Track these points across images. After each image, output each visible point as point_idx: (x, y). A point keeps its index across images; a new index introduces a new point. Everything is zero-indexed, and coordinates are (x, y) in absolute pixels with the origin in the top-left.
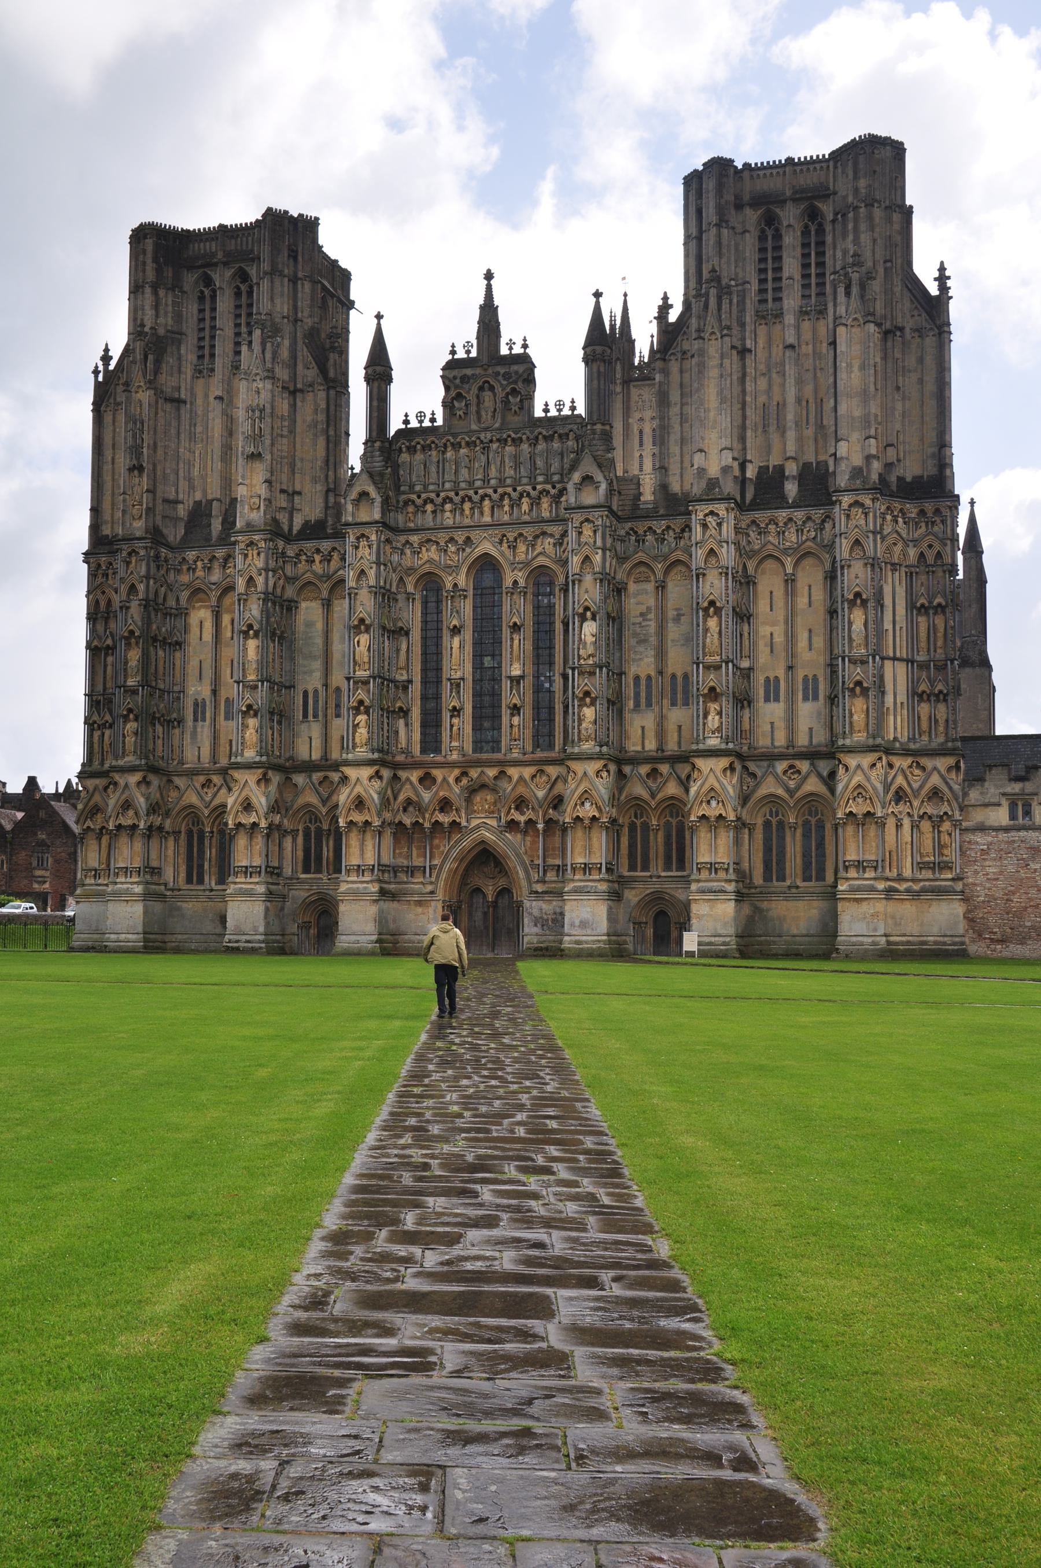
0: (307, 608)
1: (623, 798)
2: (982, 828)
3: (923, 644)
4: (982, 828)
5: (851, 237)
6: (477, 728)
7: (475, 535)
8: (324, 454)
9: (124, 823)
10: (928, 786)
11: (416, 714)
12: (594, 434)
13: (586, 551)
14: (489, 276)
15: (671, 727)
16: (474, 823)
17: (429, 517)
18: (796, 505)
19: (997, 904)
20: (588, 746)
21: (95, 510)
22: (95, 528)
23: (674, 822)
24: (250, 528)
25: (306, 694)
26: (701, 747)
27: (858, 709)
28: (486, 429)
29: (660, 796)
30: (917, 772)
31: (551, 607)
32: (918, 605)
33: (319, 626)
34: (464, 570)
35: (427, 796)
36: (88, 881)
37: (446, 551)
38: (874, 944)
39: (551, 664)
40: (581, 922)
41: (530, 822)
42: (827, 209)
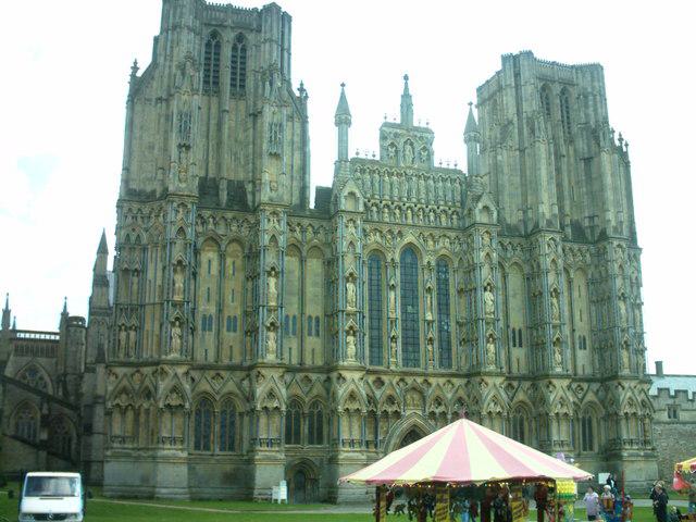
0: (288, 261)
2: (659, 423)
4: (659, 423)
5: (592, 109)
7: (405, 230)
8: (299, 162)
9: (173, 403)
11: (367, 339)
13: (487, 249)
14: (406, 78)
15: (514, 359)
16: (408, 413)
17: (375, 216)
18: (574, 241)
20: (492, 368)
21: (126, 169)
22: (126, 181)
23: (518, 416)
24: (271, 203)
25: (287, 317)
27: (624, 354)
28: (410, 168)
29: (515, 400)
31: (447, 280)
33: (297, 273)
34: (398, 251)
35: (378, 393)
36: (115, 445)
39: (448, 315)
41: (444, 414)
42: (574, 92)
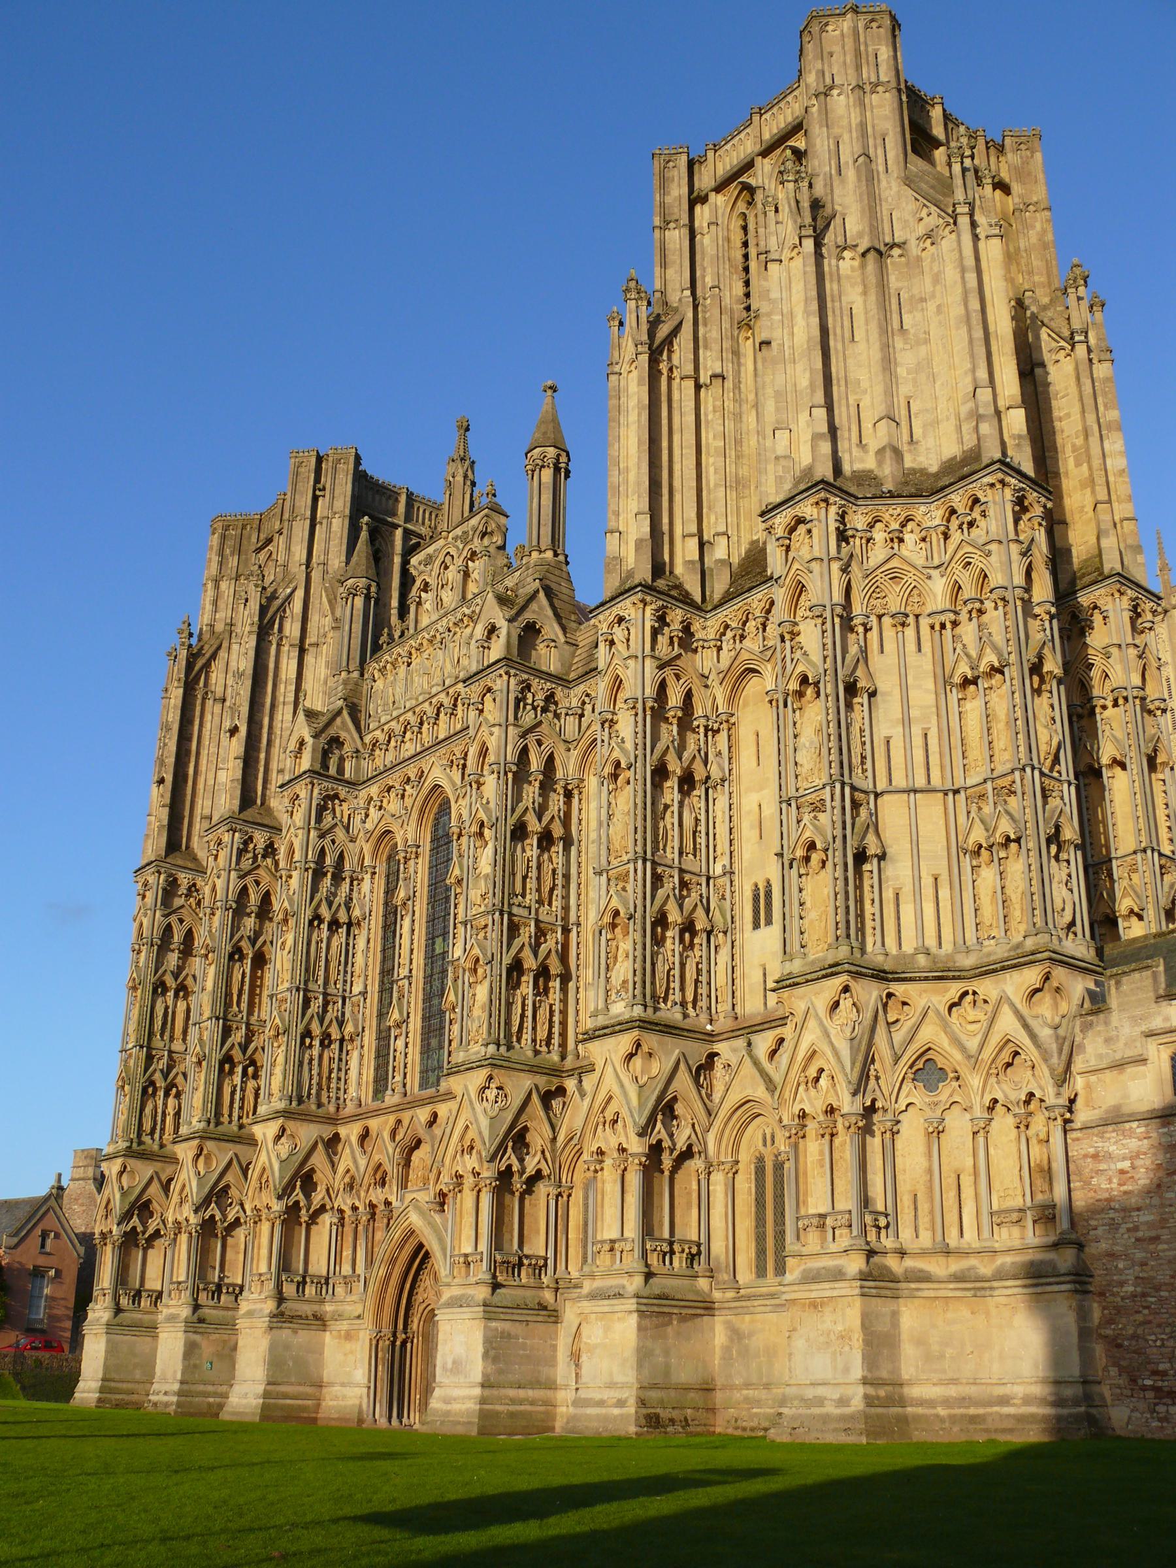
1: (561, 1138)
3: (976, 752)
6: (426, 1050)
10: (995, 1040)
12: (528, 569)
19: (1161, 1300)
26: (601, 1021)
30: (972, 1014)
32: (957, 679)
37: (403, 796)
38: (843, 1402)
40: (454, 1362)
